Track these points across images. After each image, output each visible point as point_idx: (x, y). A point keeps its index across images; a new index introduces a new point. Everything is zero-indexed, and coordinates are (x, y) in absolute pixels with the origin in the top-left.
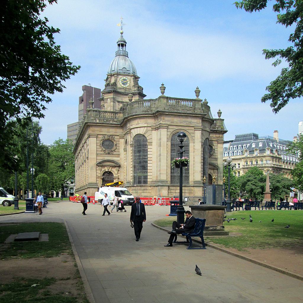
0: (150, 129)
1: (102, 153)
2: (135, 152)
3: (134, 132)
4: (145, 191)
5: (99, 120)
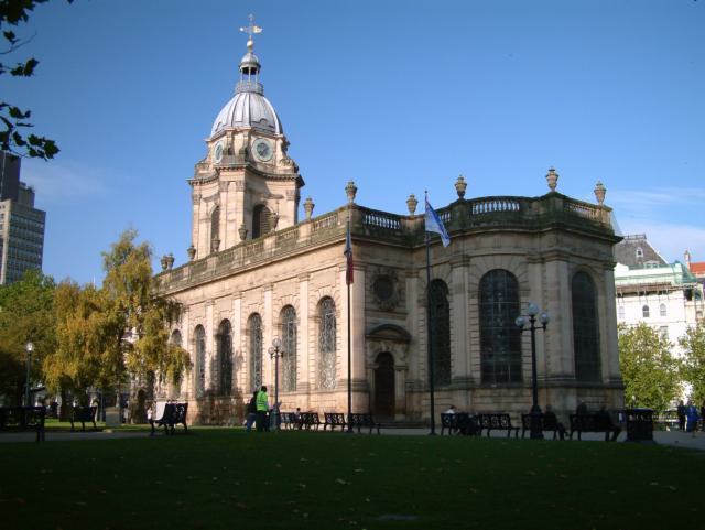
0: (524, 259)
1: (374, 307)
2: (484, 311)
3: (483, 266)
4: (521, 399)
5: (370, 231)
